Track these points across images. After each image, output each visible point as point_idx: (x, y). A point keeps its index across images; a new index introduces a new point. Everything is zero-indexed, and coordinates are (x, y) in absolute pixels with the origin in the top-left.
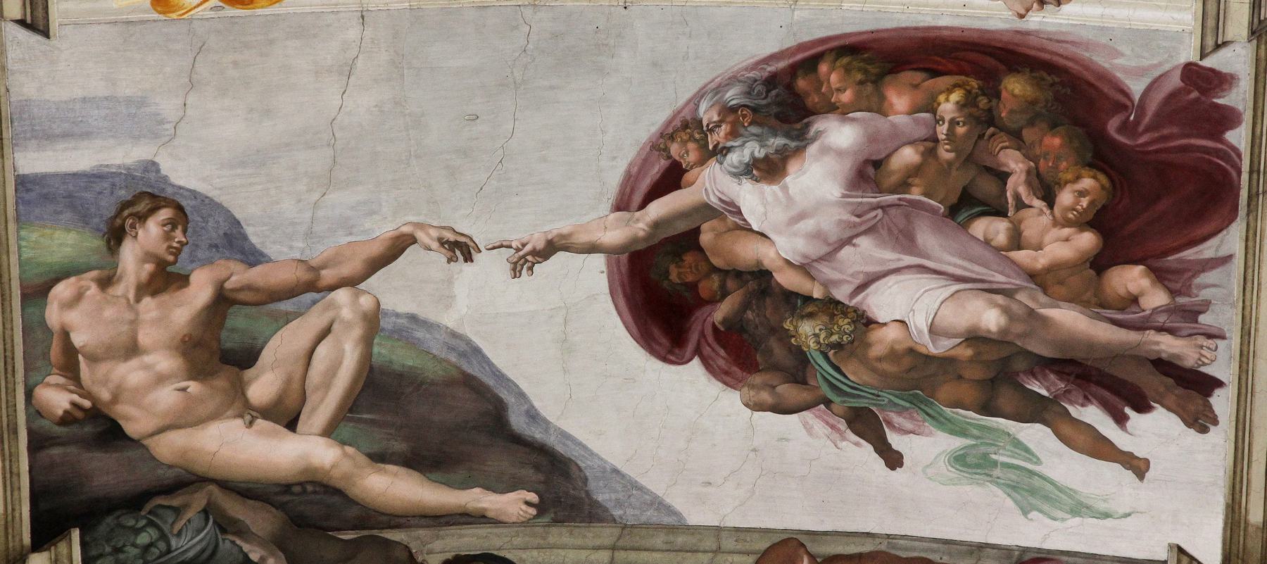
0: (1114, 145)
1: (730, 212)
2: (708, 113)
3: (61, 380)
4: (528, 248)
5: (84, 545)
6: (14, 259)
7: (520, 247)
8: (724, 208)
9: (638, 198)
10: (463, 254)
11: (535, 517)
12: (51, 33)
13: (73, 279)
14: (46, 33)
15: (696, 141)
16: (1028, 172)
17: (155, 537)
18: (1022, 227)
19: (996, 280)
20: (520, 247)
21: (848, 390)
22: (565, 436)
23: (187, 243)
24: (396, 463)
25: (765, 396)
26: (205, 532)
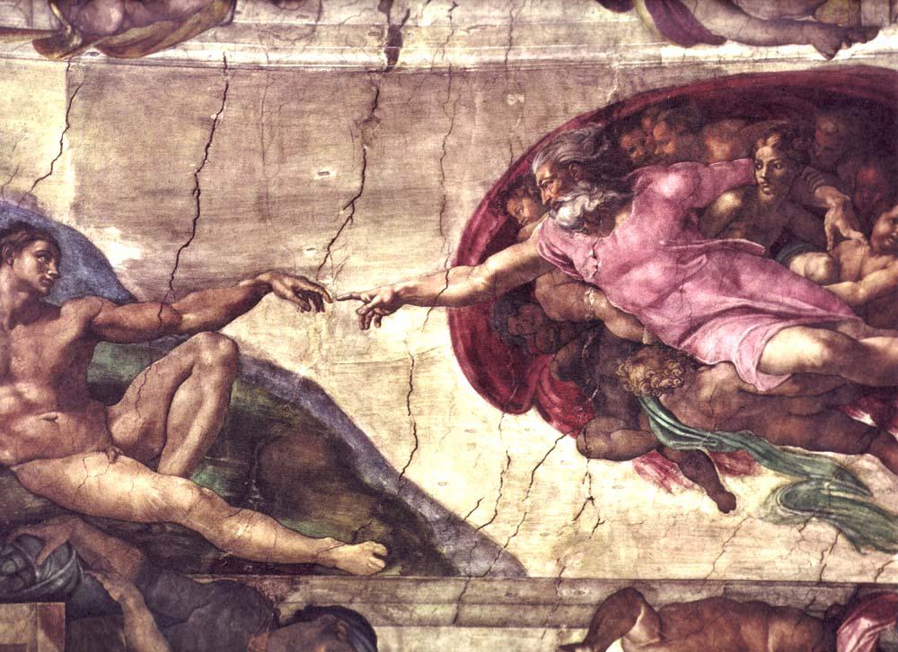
4: (376, 300)
7: (369, 299)
10: (315, 303)
11: (384, 570)
15: (529, 196)
16: (844, 206)
18: (843, 257)
20: (369, 299)
21: (678, 432)
26: (69, 565)
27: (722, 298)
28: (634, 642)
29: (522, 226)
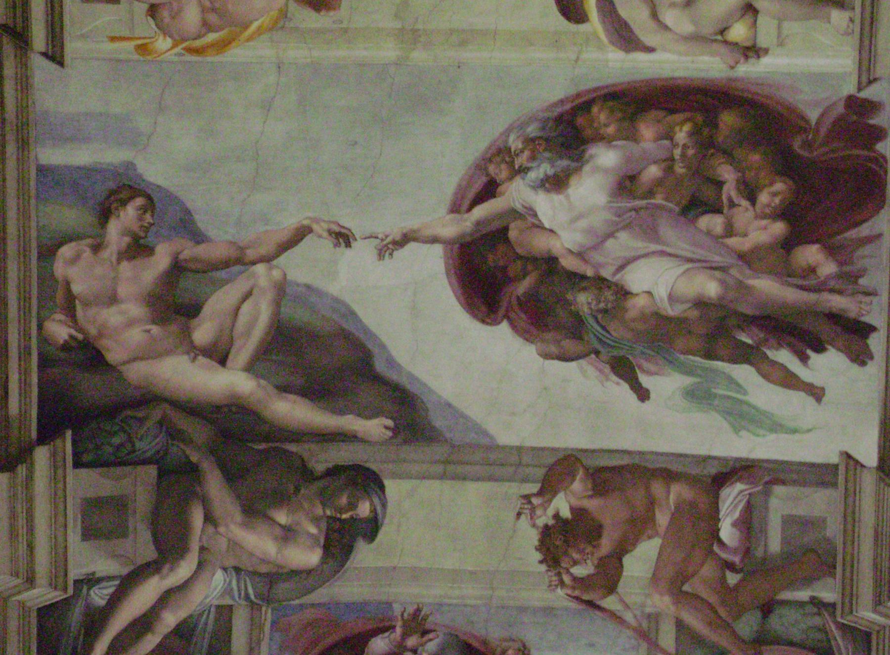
0: (799, 157)
1: (529, 214)
2: (515, 143)
3: (62, 317)
4: (389, 239)
5: (74, 442)
6: (33, 224)
7: (384, 238)
8: (527, 213)
9: (466, 203)
11: (391, 438)
12: (65, 64)
13: (73, 244)
14: (61, 64)
16: (738, 181)
17: (124, 439)
19: (714, 260)
20: (384, 238)
21: (613, 344)
22: (413, 378)
23: (153, 224)
24: (295, 394)
25: (553, 349)
27: (646, 245)
28: (574, 494)
29: (498, 185)
